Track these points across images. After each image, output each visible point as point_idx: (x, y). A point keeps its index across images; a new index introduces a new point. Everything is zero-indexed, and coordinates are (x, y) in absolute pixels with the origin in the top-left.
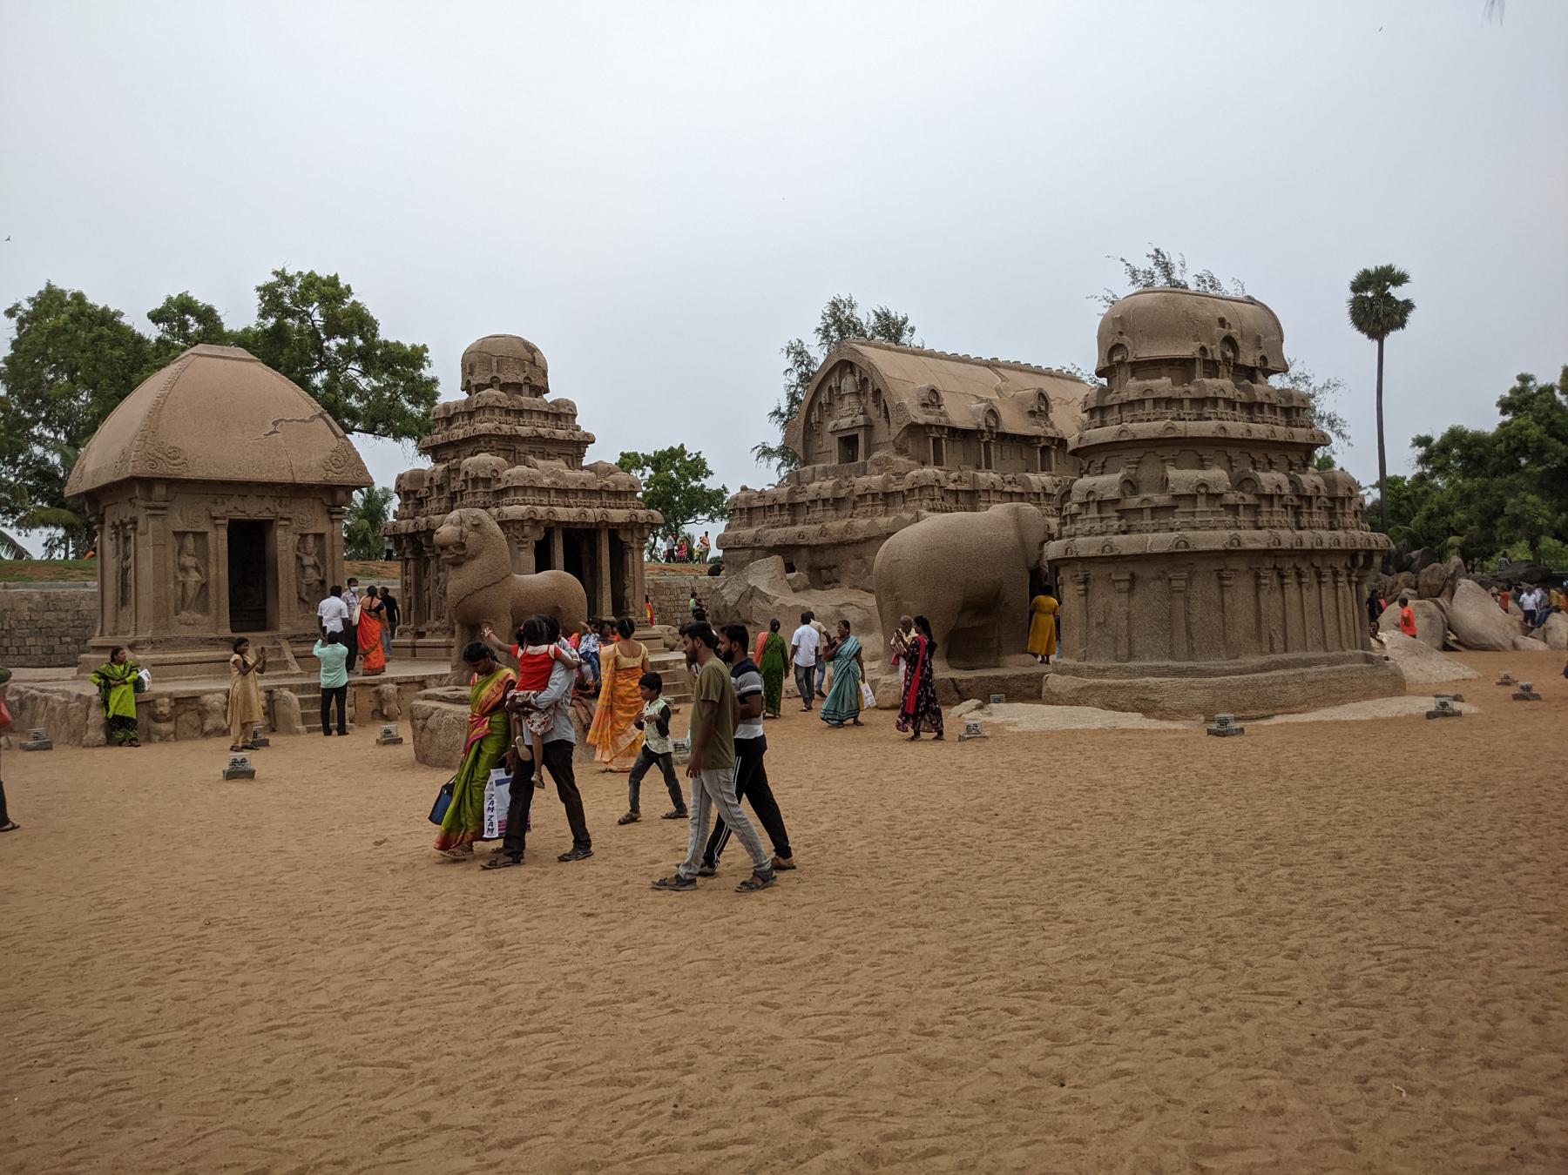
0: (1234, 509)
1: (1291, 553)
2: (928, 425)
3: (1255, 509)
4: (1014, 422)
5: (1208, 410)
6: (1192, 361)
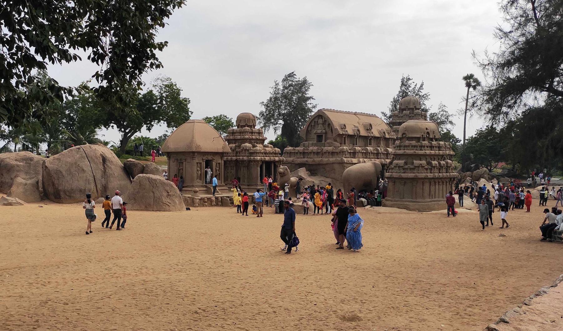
0: (427, 169)
1: (438, 178)
2: (343, 134)
3: (431, 169)
4: (363, 133)
5: (423, 148)
6: (420, 138)
